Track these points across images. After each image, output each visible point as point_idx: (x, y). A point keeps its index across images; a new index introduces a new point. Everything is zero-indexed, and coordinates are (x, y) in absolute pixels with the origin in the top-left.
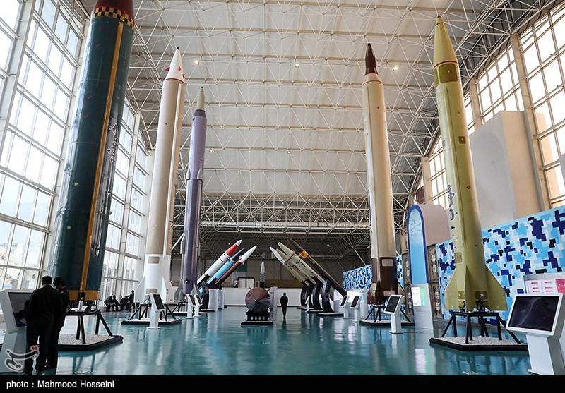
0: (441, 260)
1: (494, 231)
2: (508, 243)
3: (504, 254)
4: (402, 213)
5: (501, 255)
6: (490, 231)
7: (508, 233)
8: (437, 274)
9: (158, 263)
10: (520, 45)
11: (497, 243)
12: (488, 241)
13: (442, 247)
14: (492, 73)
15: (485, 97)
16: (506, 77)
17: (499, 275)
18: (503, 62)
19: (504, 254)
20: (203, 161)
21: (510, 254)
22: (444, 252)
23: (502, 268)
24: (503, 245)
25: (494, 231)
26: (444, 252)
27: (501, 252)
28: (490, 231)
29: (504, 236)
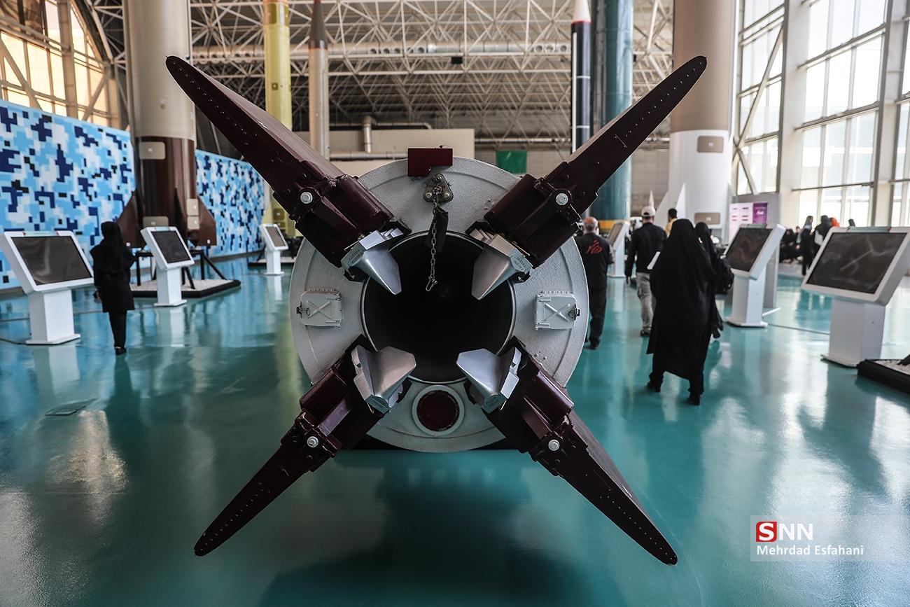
2: (125, 159)
3: (118, 171)
5: (115, 172)
7: (125, 146)
11: (109, 153)
12: (97, 144)
17: (109, 199)
19: (118, 171)
21: (126, 174)
23: (115, 191)
24: (118, 162)
27: (114, 168)
29: (120, 148)
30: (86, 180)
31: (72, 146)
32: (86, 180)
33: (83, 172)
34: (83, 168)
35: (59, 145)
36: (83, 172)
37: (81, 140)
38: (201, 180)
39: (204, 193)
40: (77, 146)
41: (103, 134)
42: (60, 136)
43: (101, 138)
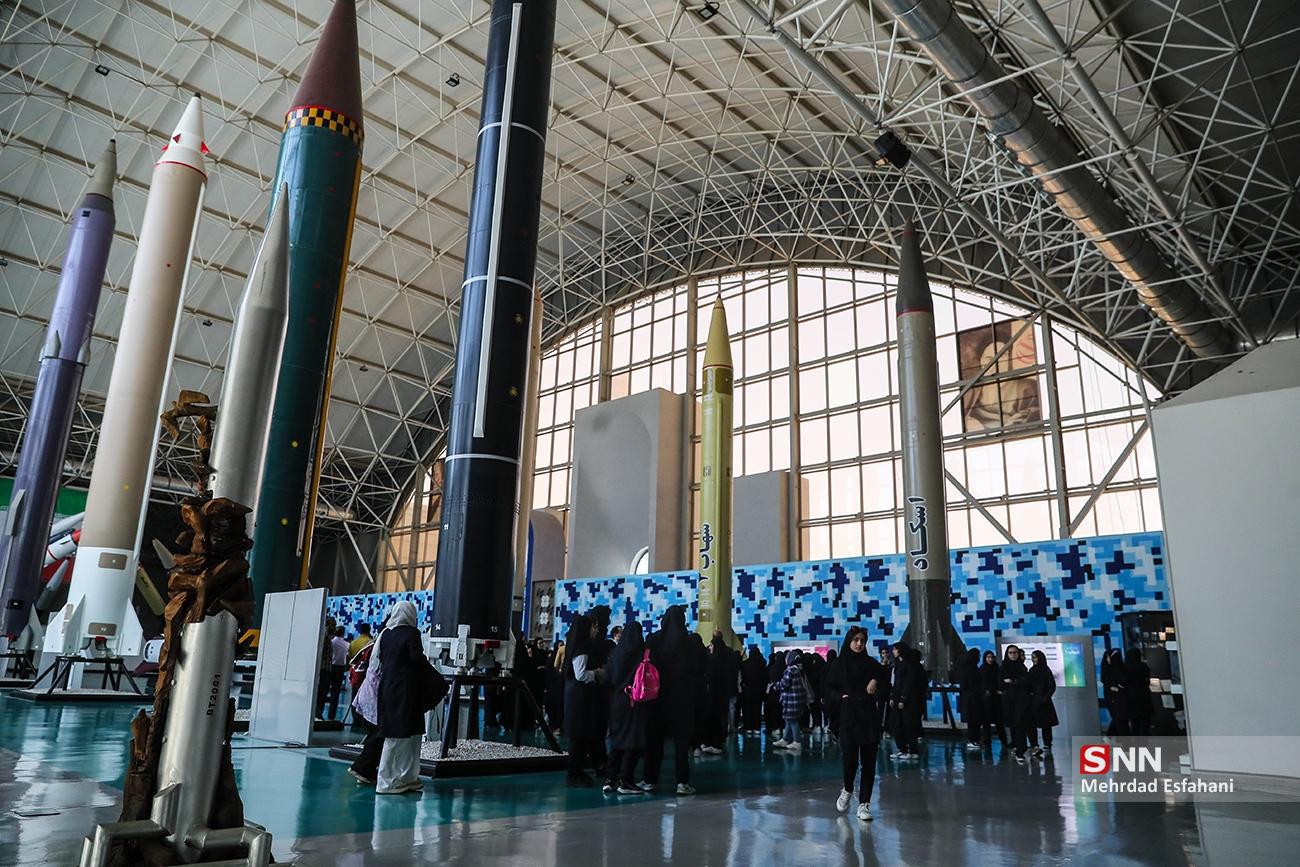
0: (564, 607)
1: (678, 578)
4: (390, 498)
6: (672, 576)
8: (550, 626)
9: (123, 569)
10: (696, 288)
11: (680, 594)
12: (666, 589)
13: (568, 587)
14: (643, 316)
15: (620, 345)
16: (663, 330)
18: (664, 308)
20: (93, 320)
22: (574, 595)
25: (678, 578)
26: (574, 595)
28: (672, 576)
30: (651, 622)
31: (640, 595)
32: (651, 622)
33: (648, 616)
34: (649, 612)
35: (629, 599)
36: (648, 616)
37: (650, 589)
38: (855, 597)
39: (863, 617)
40: (645, 595)
41: (675, 579)
42: (630, 591)
43: (671, 582)
